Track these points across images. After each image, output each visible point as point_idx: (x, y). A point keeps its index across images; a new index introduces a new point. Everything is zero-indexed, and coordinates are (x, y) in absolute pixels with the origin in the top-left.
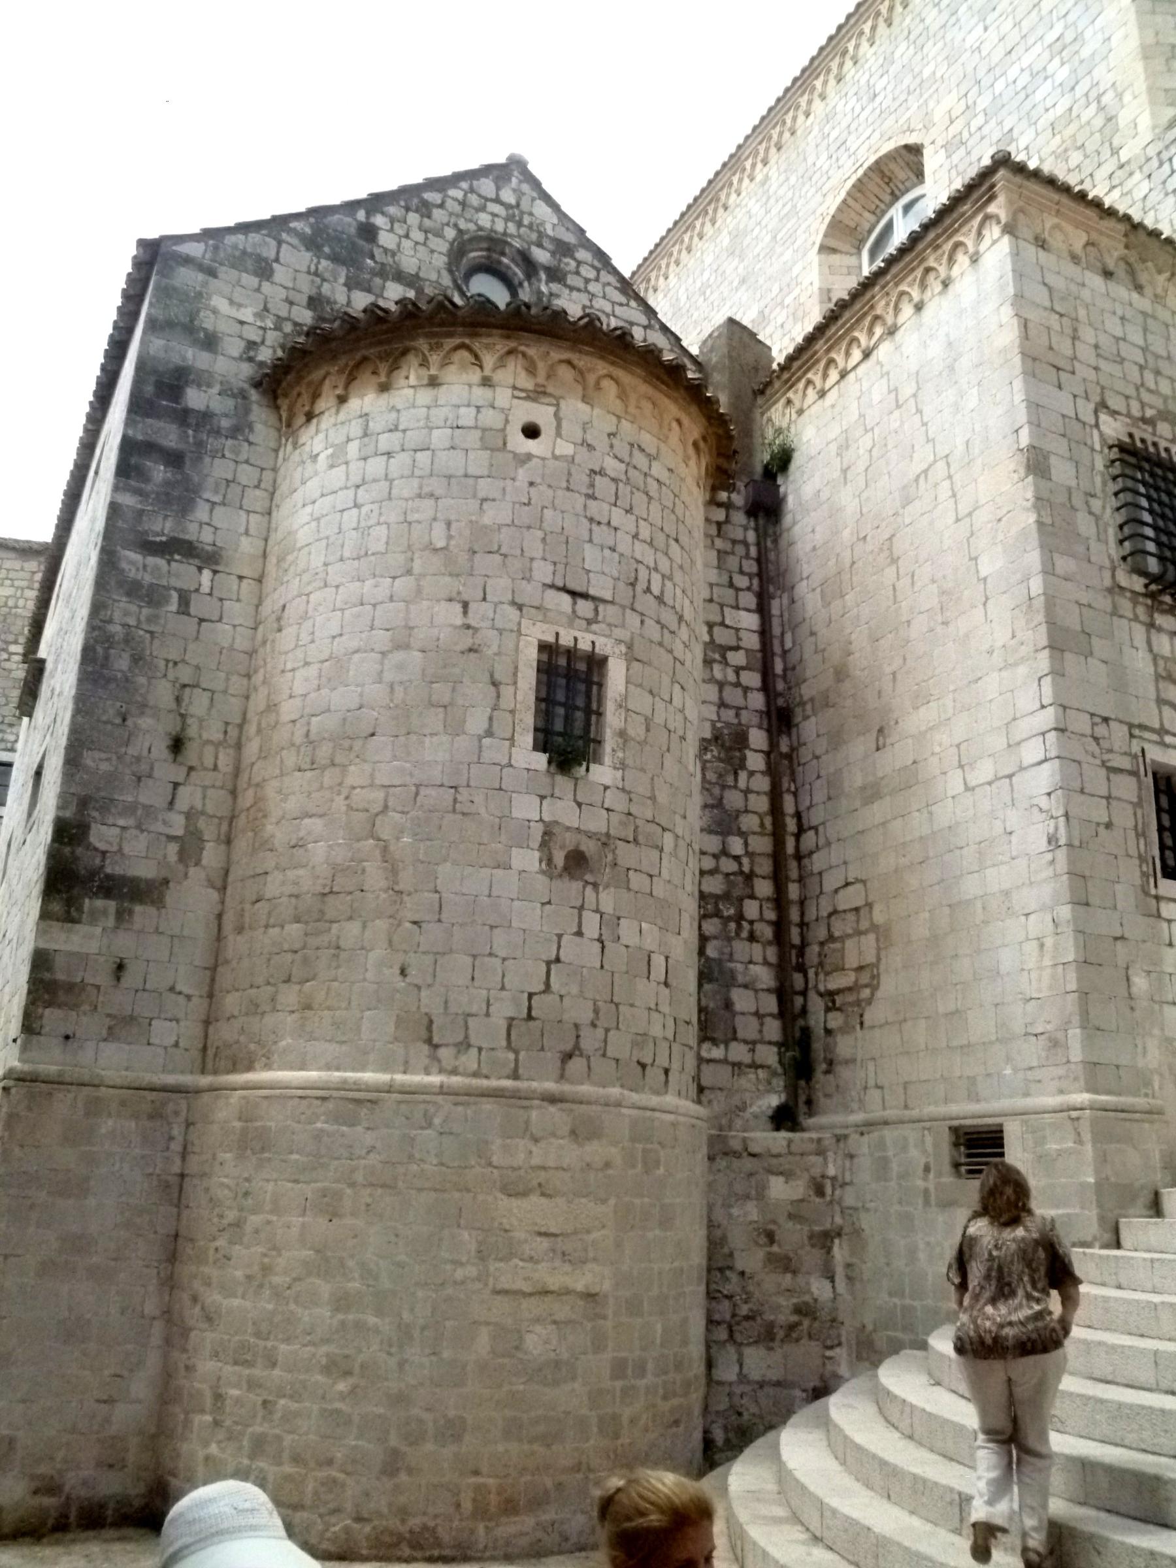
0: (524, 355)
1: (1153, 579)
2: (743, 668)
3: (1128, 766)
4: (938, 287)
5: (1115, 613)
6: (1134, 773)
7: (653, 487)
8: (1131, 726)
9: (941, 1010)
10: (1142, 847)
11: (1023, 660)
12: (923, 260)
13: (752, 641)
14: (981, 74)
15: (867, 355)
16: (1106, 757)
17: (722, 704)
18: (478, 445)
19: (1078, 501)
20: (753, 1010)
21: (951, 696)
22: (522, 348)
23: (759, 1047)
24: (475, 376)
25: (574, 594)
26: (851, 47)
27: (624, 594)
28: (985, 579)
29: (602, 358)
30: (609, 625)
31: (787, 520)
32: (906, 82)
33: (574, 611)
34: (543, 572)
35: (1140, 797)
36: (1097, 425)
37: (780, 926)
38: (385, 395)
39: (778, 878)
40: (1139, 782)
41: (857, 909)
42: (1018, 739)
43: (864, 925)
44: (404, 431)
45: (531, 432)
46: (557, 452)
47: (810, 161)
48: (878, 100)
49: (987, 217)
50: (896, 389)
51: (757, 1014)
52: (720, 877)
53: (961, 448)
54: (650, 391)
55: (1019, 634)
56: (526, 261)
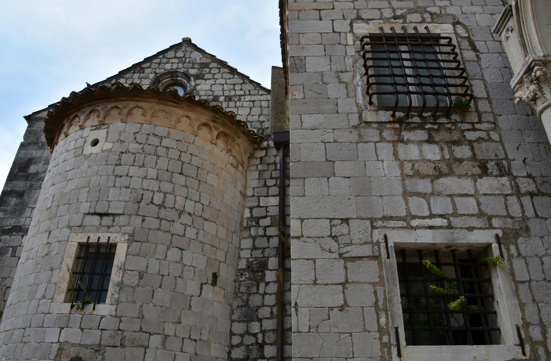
2: (268, 226)
3: (369, 253)
5: (361, 139)
6: (376, 257)
7: (161, 151)
8: (372, 220)
10: (383, 320)
13: (275, 211)
16: (343, 250)
17: (254, 248)
25: (101, 215)
27: (132, 207)
29: (132, 100)
34: (85, 207)
35: (381, 277)
36: (352, 31)
40: (380, 264)
45: (95, 143)
52: (243, 348)
54: (162, 107)
56: (187, 76)
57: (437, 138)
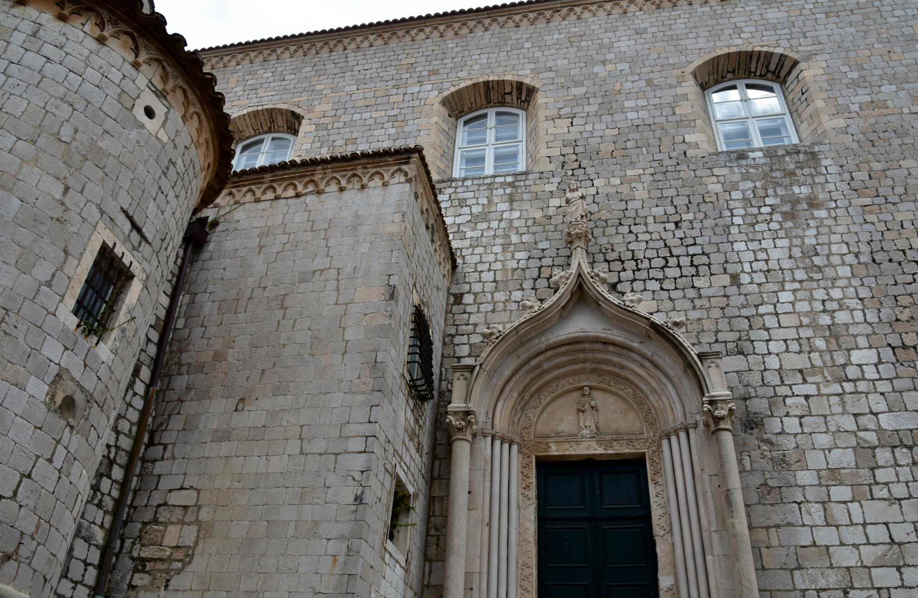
0: (164, 68)
1: (412, 380)
4: (358, 186)
9: (242, 588)
11: (363, 393)
12: (354, 169)
14: (349, 105)
15: (298, 196)
18: (116, 97)
19: (402, 324)
20: (83, 558)
21: (304, 396)
22: (165, 64)
23: (79, 586)
24: (131, 57)
26: (279, 51)
28: (348, 341)
29: (201, 104)
30: (143, 257)
31: (205, 255)
32: (305, 85)
33: (129, 236)
34: (125, 200)
37: (119, 503)
38: (62, 24)
39: (128, 469)
41: (185, 508)
42: (348, 434)
43: (190, 518)
44: (67, 54)
45: (150, 113)
46: (159, 136)
47: (230, 85)
48: (284, 83)
49: (400, 170)
50: (313, 221)
51: (85, 562)
53: (349, 269)
55: (363, 378)
57: (415, 412)
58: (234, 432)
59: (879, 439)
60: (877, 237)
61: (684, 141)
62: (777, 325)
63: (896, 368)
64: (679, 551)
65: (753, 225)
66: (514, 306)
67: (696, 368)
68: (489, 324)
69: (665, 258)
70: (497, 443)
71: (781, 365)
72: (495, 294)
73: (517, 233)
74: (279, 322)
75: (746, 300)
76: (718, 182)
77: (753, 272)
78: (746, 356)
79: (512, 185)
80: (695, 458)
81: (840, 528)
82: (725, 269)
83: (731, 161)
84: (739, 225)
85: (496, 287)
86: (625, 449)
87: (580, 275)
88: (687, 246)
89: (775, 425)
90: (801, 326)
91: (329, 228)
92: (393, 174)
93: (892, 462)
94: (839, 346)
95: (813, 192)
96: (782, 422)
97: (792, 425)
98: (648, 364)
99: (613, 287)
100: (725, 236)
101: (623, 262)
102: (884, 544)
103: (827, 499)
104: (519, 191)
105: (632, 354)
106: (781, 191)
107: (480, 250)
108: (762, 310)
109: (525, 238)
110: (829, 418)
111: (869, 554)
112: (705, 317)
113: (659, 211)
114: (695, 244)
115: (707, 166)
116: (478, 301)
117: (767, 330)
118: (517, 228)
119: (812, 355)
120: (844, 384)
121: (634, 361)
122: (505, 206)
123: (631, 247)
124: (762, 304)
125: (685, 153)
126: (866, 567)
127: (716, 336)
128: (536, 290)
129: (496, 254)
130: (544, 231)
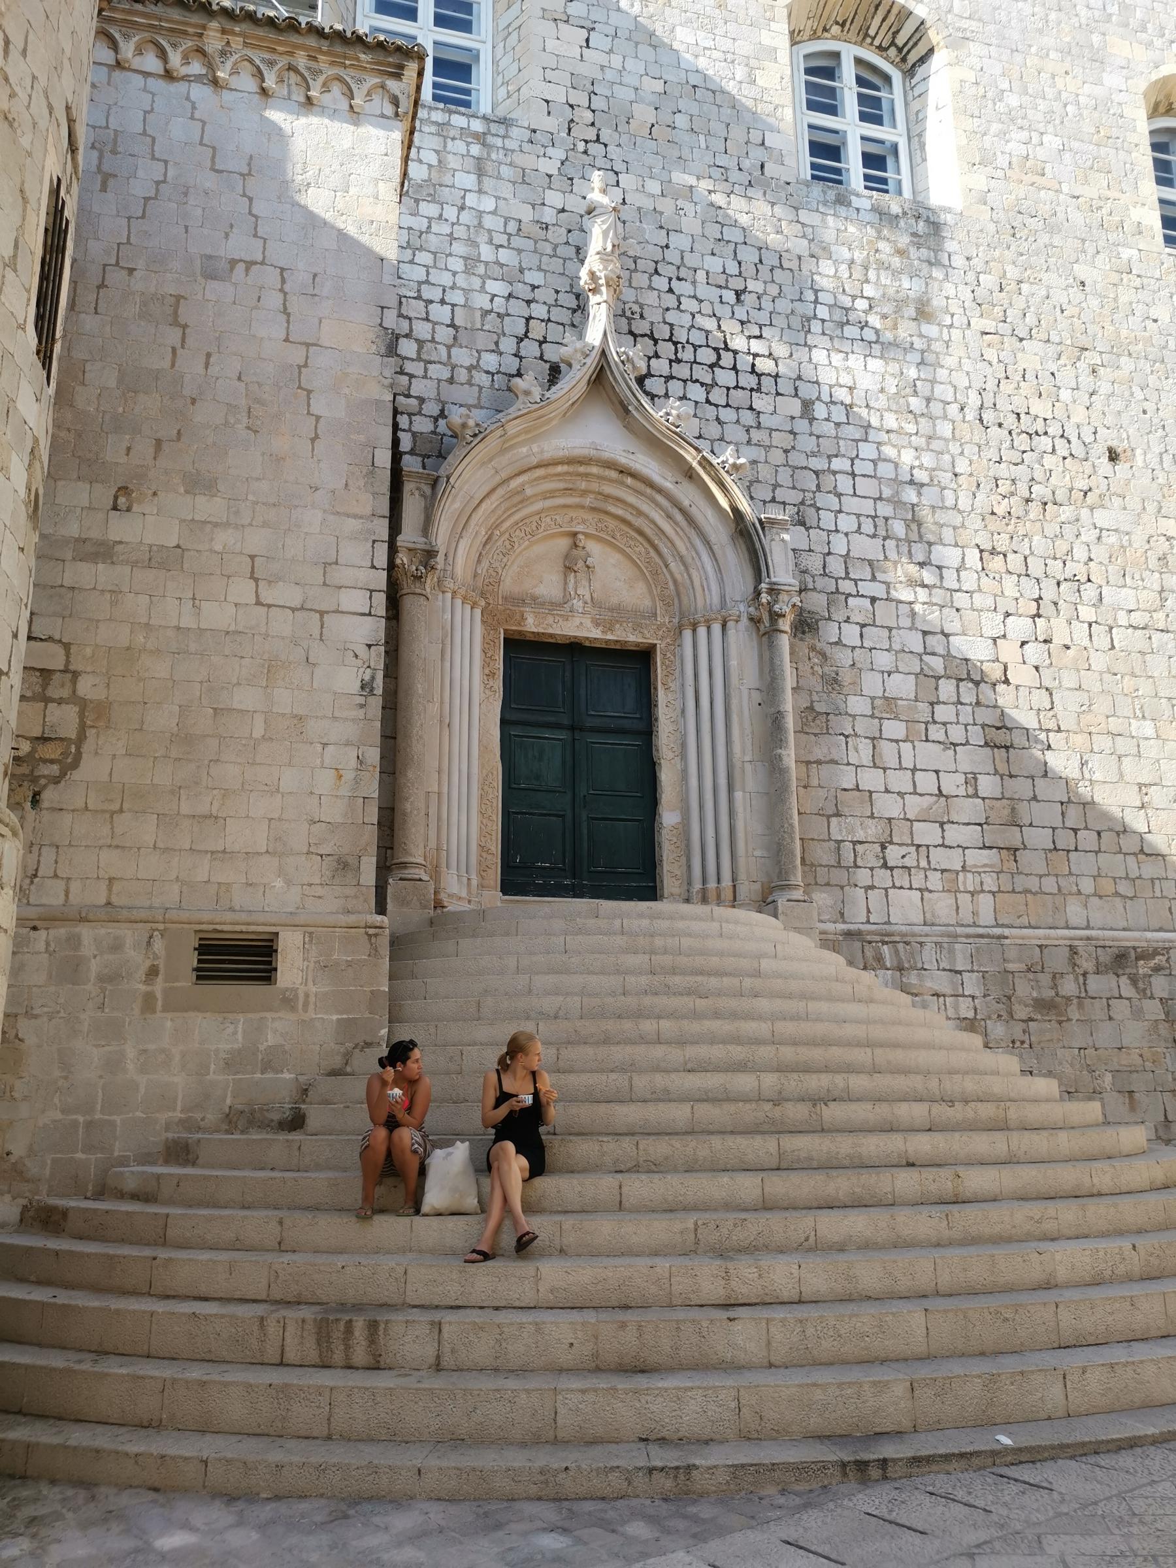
11: (355, 516)
28: (318, 418)
49: (383, 87)
58: (119, 548)
59: (945, 668)
60: (991, 385)
61: (763, 144)
62: (851, 492)
63: (979, 578)
64: (693, 782)
65: (842, 325)
66: (485, 380)
67: (755, 538)
68: (444, 403)
69: (716, 349)
70: (459, 602)
71: (849, 550)
72: (454, 351)
73: (490, 242)
74: (174, 350)
75: (818, 446)
76: (804, 236)
77: (832, 402)
78: (807, 529)
79: (481, 138)
80: (734, 663)
81: (888, 771)
82: (796, 389)
83: (825, 203)
84: (823, 321)
85: (455, 338)
86: (629, 636)
87: (603, 353)
88: (749, 337)
89: (830, 631)
90: (880, 498)
91: (250, 174)
92: (369, 94)
93: (955, 699)
94: (921, 537)
95: (926, 293)
96: (840, 628)
97: (851, 634)
98: (679, 517)
99: (640, 381)
100: (803, 334)
101: (656, 341)
102: (931, 795)
103: (878, 735)
104: (494, 156)
105: (659, 498)
106: (886, 279)
107: (424, 258)
108: (837, 464)
109: (505, 256)
110: (894, 632)
111: (914, 805)
112: (762, 459)
113: (714, 264)
114: (761, 337)
115: (792, 201)
116: (424, 356)
117: (839, 495)
118: (489, 231)
119: (888, 542)
120: (918, 589)
121: (657, 504)
122: (470, 181)
123: (671, 317)
124: (836, 456)
125: (762, 166)
126: (908, 820)
127: (773, 491)
128: (521, 358)
129: (455, 274)
130: (535, 251)
